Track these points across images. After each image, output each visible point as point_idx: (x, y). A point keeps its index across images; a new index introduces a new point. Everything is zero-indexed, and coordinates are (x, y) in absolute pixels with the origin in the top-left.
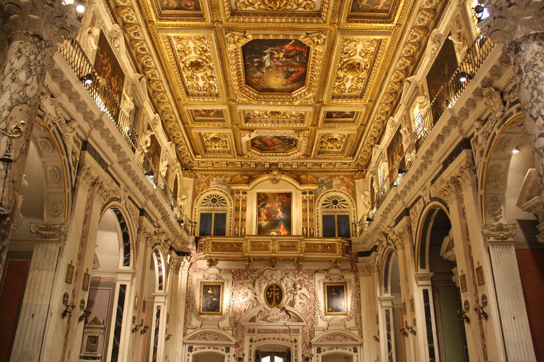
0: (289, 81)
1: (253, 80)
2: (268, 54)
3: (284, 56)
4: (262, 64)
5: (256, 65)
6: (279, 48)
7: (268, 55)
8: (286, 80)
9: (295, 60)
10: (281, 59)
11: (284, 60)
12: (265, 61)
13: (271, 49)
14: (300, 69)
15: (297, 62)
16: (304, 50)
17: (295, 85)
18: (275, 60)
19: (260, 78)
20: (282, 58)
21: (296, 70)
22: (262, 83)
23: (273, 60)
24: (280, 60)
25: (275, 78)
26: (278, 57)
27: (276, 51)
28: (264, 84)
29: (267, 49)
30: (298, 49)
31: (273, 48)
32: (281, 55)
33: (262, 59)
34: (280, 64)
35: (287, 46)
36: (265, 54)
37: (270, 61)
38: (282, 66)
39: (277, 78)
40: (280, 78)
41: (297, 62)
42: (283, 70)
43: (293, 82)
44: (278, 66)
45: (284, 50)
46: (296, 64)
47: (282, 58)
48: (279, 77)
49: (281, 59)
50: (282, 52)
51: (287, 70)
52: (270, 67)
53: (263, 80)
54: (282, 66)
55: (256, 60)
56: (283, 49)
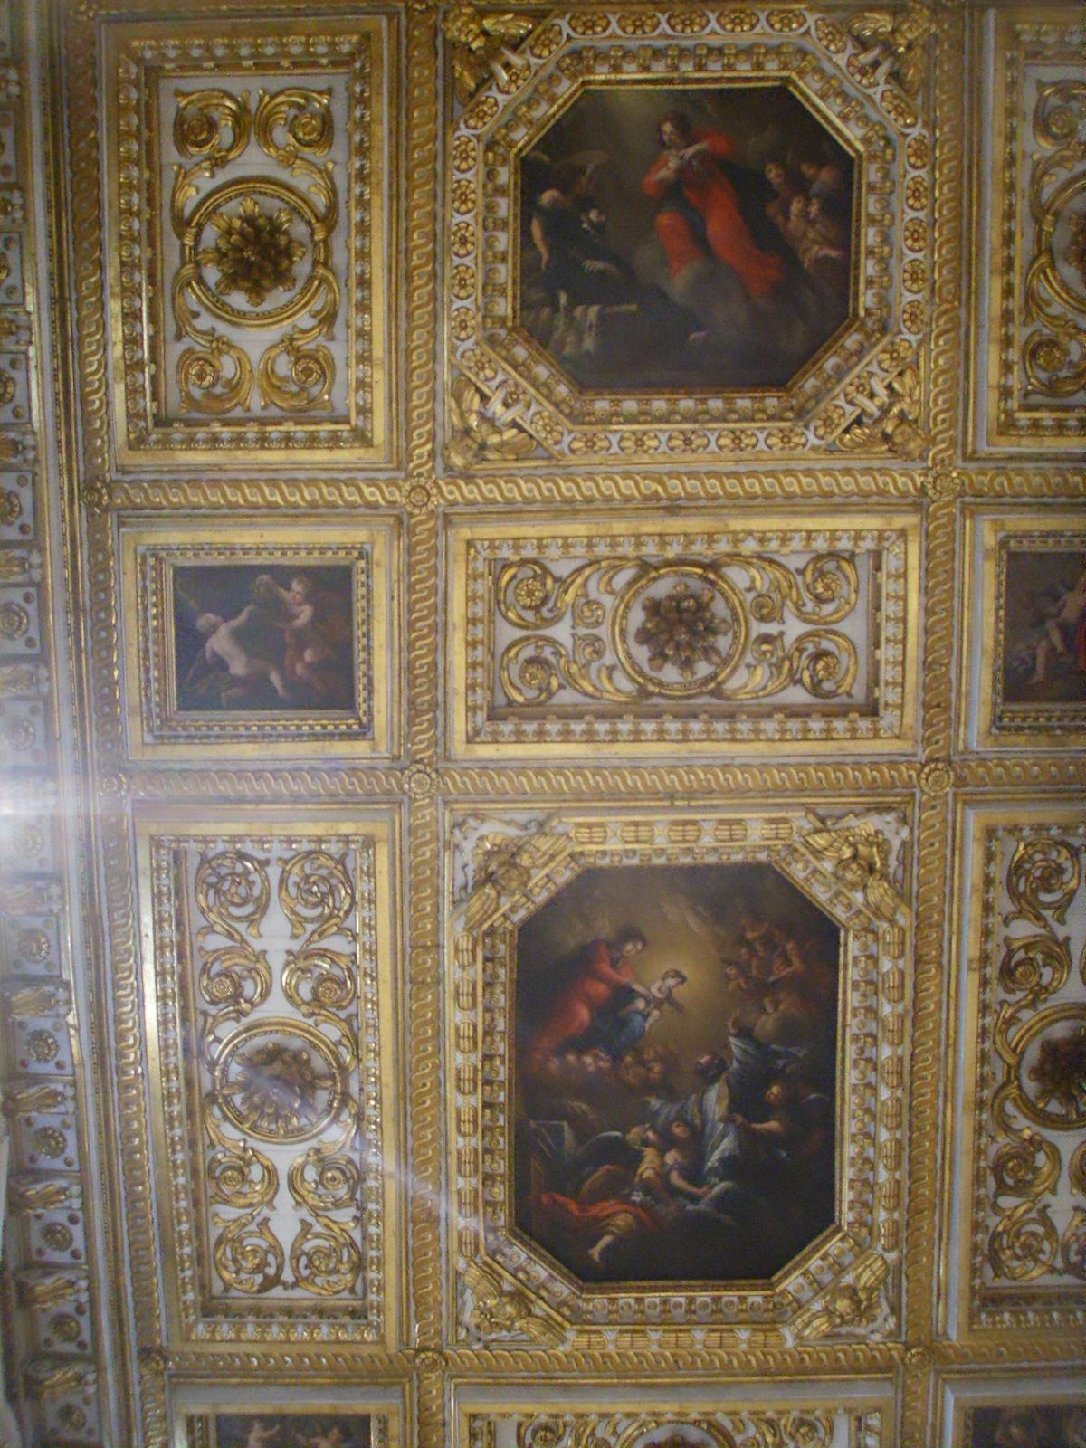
0: (605, 968)
1: (797, 963)
2: (713, 1171)
3: (638, 1158)
4: (746, 1103)
5: (775, 1090)
6: (658, 1207)
7: (713, 1160)
8: (624, 978)
9: (580, 1136)
10: (650, 1134)
11: (634, 1133)
12: (728, 1120)
13: (694, 1199)
14: (554, 1064)
15: (573, 1120)
16: (545, 1199)
17: (571, 938)
18: (678, 1130)
19: (761, 990)
20: (646, 1143)
21: (571, 1058)
22: (749, 944)
23: (688, 1125)
24: (652, 1128)
25: (681, 993)
26: (662, 1153)
27: (674, 1192)
28: (742, 941)
29: (720, 1202)
30: (573, 1207)
31: (690, 1207)
32: (648, 1167)
33: (748, 1138)
34: (655, 1103)
35: (623, 1220)
36: (730, 1166)
37: (704, 1123)
38: (649, 1088)
39: (669, 998)
40: (654, 990)
41: (573, 1120)
42: (641, 1062)
43: (583, 961)
44: (667, 1090)
45: (637, 1197)
46: (581, 1106)
47: (646, 1143)
48: (659, 1004)
49: (650, 1134)
50: (647, 1188)
51: (616, 1058)
52: (707, 1076)
53: (743, 969)
54: (649, 1088)
55: (773, 1125)
56: (642, 1205)
